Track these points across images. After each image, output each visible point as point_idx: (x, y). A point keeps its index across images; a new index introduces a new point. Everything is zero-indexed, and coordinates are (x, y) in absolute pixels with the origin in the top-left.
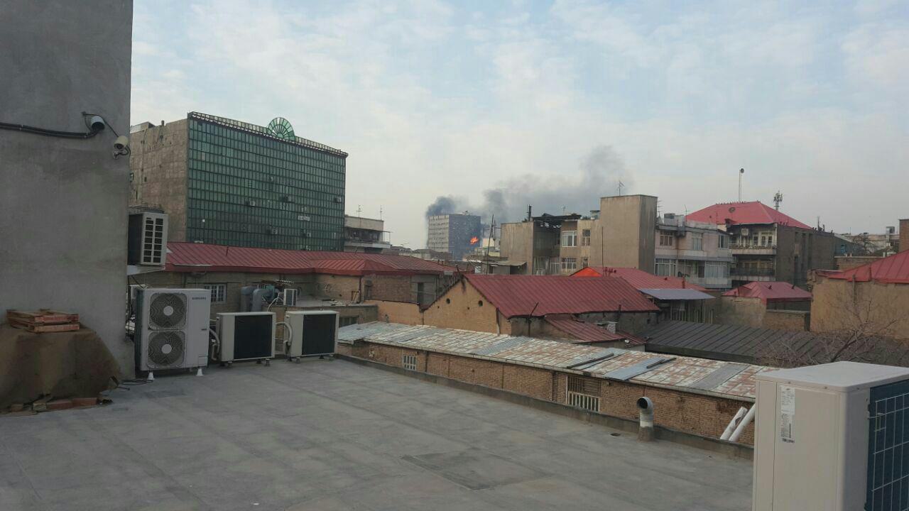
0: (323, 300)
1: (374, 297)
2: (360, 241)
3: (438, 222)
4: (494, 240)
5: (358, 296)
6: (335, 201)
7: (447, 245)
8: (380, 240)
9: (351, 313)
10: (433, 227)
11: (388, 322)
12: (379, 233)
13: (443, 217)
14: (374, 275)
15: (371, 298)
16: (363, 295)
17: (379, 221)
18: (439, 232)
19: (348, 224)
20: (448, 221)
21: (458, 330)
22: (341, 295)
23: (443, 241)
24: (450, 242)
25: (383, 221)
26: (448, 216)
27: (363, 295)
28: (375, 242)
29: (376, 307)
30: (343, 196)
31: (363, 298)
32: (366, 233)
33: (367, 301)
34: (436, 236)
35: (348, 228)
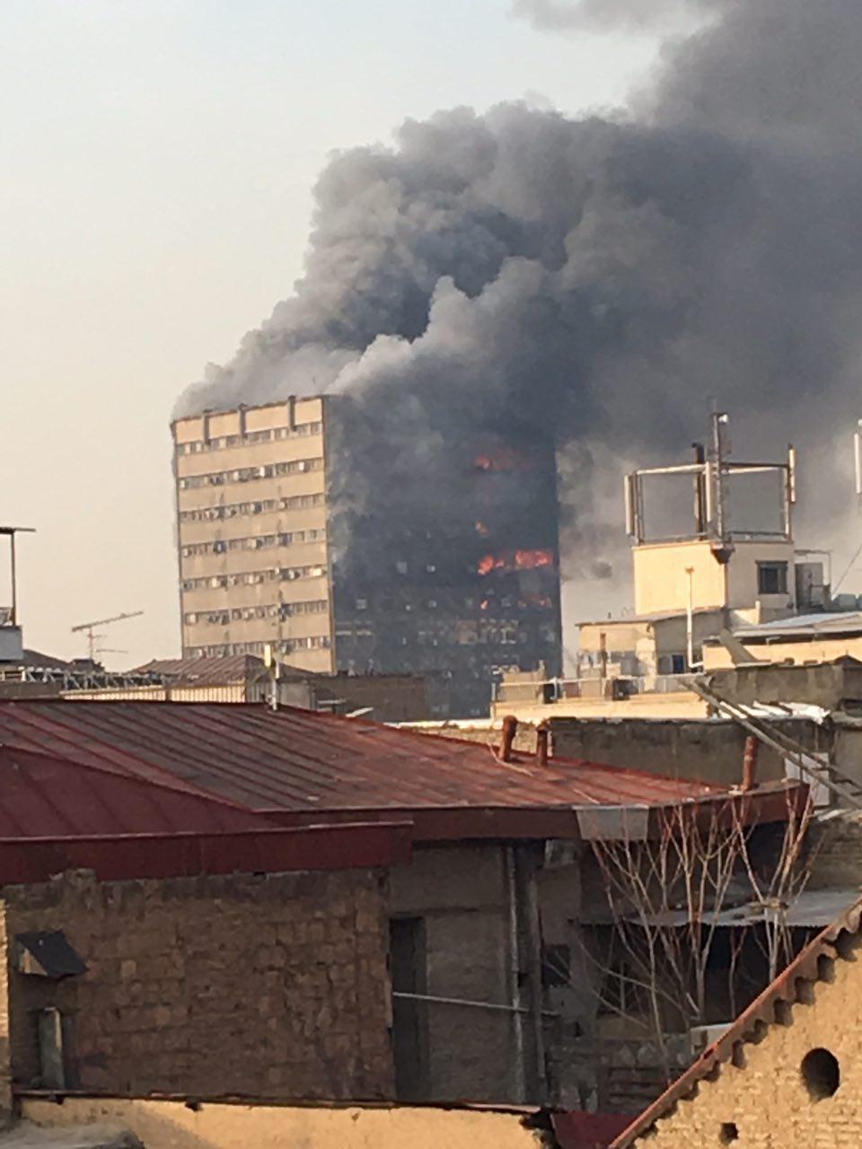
1: (91, 1075)
3: (242, 457)
4: (721, 556)
7: (319, 624)
13: (280, 417)
14: (82, 879)
18: (258, 526)
20: (313, 446)
23: (292, 593)
24: (342, 601)
26: (310, 413)
33: (33, 1108)
34: (235, 562)
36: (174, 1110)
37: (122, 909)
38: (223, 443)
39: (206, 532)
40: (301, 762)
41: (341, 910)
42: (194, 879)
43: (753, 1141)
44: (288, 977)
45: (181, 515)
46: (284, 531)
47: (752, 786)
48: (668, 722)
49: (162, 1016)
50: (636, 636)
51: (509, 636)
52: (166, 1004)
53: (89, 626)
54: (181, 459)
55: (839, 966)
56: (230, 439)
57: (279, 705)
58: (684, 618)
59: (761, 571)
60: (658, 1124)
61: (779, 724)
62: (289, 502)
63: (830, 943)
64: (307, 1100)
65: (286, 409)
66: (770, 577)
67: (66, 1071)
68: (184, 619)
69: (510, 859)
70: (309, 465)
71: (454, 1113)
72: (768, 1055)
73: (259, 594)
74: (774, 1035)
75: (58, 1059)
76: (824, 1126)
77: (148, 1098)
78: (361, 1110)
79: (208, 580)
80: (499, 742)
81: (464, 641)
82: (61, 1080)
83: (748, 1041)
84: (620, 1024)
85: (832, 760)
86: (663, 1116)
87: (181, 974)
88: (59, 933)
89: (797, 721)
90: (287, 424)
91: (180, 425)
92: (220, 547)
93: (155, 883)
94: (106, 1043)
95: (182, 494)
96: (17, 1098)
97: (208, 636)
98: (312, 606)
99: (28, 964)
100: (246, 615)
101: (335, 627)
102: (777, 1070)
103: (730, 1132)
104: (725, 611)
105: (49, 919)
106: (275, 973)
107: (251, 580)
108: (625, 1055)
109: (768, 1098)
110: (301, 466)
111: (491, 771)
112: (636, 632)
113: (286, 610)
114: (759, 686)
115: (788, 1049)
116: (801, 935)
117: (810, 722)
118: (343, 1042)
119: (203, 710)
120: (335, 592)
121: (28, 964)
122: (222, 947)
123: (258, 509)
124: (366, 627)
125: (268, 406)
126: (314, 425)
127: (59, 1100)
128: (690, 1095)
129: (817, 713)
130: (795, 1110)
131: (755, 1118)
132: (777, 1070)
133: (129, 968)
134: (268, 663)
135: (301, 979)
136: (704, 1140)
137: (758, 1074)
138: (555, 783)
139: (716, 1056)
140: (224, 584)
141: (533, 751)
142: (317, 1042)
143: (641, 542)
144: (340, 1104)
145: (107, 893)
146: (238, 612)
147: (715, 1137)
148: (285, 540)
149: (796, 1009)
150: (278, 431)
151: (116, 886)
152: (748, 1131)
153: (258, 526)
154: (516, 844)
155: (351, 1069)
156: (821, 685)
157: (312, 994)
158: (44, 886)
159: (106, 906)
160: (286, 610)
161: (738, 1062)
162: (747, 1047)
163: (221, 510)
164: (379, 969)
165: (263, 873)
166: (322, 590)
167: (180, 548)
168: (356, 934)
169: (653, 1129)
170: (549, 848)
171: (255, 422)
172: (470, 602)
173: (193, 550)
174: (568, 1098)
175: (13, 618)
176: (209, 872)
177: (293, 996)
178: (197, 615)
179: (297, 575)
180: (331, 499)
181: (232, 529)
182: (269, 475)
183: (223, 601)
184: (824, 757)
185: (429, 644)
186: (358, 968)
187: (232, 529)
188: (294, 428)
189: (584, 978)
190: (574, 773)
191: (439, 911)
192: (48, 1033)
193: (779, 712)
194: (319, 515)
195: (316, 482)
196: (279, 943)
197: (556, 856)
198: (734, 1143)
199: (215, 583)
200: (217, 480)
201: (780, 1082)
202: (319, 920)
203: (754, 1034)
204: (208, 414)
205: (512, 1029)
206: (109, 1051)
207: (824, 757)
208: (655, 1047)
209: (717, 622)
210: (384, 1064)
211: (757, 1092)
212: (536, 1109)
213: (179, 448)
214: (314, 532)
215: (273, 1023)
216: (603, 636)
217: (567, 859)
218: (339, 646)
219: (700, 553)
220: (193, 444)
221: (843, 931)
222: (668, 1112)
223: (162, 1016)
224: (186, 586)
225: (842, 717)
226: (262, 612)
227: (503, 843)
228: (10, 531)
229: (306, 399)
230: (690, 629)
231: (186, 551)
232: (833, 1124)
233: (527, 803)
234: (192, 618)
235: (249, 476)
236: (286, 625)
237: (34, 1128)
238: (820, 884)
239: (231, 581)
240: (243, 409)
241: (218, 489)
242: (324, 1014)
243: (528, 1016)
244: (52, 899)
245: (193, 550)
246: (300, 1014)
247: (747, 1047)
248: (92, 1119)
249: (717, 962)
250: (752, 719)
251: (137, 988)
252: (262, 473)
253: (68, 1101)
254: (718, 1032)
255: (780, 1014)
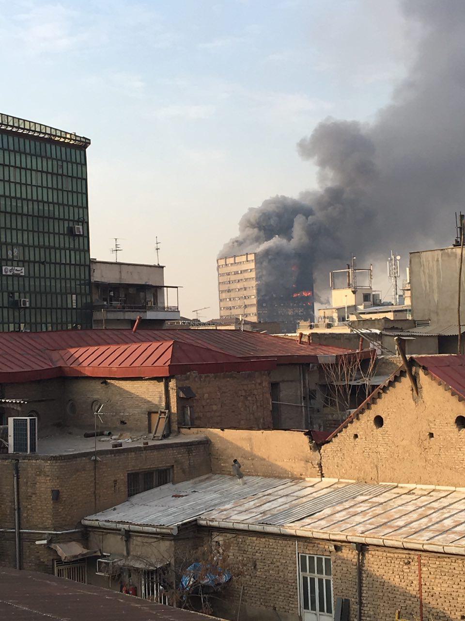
0: (87, 436)
1: (197, 422)
2: (123, 309)
3: (235, 268)
4: (354, 292)
5: (163, 423)
6: (71, 232)
7: (254, 310)
8: (159, 305)
9: (156, 461)
10: (225, 278)
11: (241, 476)
12: (157, 290)
13: (244, 258)
14: (194, 374)
15: (193, 425)
16: (174, 418)
17: (154, 266)
18: (239, 286)
19: (98, 276)
20: (252, 265)
21: (411, 486)
22: (123, 423)
23: (247, 302)
24: (260, 304)
25: (163, 267)
26: (251, 257)
27: (174, 418)
28: (151, 309)
29: (206, 443)
30: (85, 223)
31: (175, 426)
32: (131, 291)
33: (183, 430)
34: (233, 294)
35: (98, 285)
36: (217, 431)
37: (204, 381)
38: (230, 265)
39: (226, 287)
40: (249, 344)
41: (259, 381)
42: (222, 374)
43: (362, 438)
44: (246, 398)
45: (219, 283)
46: (245, 286)
47: (362, 350)
48: (340, 334)
49: (215, 408)
50: (333, 312)
51: (301, 312)
52: (216, 405)
53: (197, 311)
54: (220, 269)
55: (383, 395)
56: (232, 264)
57: (244, 330)
58: (345, 308)
59: (364, 296)
60: (338, 434)
61: (368, 334)
62: (246, 279)
63: (381, 389)
64: (251, 429)
65: (246, 256)
66: (366, 297)
67: (191, 421)
68: (220, 308)
69: (301, 369)
70: (251, 270)
71: (287, 432)
72: (366, 417)
73: (239, 303)
74: (367, 412)
75: (189, 418)
76: (379, 435)
77: (212, 428)
78: (264, 431)
79: (226, 299)
80: (298, 339)
81: (290, 314)
82: (190, 424)
83: (360, 413)
84: (329, 409)
85: (382, 343)
86: (339, 432)
87: (219, 397)
88: (189, 387)
89: (373, 334)
90: (246, 260)
91: (219, 261)
92: (229, 291)
93: (213, 374)
94: (201, 414)
95: (220, 278)
96: (179, 428)
97: (226, 313)
98: (252, 305)
99: (182, 395)
100: (236, 308)
101: (258, 311)
102: (368, 421)
103: (356, 436)
104: (355, 306)
105: (187, 383)
106: (242, 397)
107: (237, 299)
108: (330, 417)
109: (366, 428)
110: (249, 271)
111: (297, 346)
112: (332, 311)
113: (246, 306)
114: (363, 325)
115: (371, 415)
116: (374, 387)
117: (376, 334)
118: (259, 414)
119: (224, 332)
120: (258, 302)
121: (182, 395)
122: (229, 391)
123: (239, 281)
124: (266, 311)
125: (241, 256)
126: (252, 260)
127: (189, 428)
128: (346, 427)
129: (378, 332)
130: (372, 431)
131: (362, 433)
132: (368, 421)
133: (206, 396)
134: (241, 320)
135: (249, 398)
136: (350, 438)
137: (363, 422)
138: (312, 349)
139: (352, 417)
140: (230, 300)
141: (307, 341)
142: (253, 414)
143: (334, 289)
144: (259, 429)
145: (201, 377)
146: (234, 307)
147: (352, 437)
148: (245, 289)
149: (372, 406)
150: (243, 262)
151: (203, 376)
152: (361, 436)
153: (239, 286)
154: (303, 364)
155: (262, 420)
156: (379, 324)
157: (251, 402)
158: (185, 375)
159: (200, 380)
160: (246, 306)
161: (358, 419)
162: (360, 415)
163: (229, 281)
164: (268, 396)
165: (239, 372)
166: (254, 301)
167: (219, 291)
168: (263, 387)
169: (337, 435)
170: (311, 365)
171: (238, 259)
172: (291, 304)
173: (222, 292)
174: (316, 427)
175: (178, 309)
176: (226, 371)
177: (247, 403)
178: (224, 308)
179: (248, 298)
180: (257, 279)
181: (232, 286)
182: (241, 273)
183: (230, 304)
184: (380, 342)
185: (281, 315)
186: (263, 395)
187: (232, 286)
188: (248, 261)
189: (320, 397)
190: (317, 347)
191: (283, 381)
192: (187, 412)
193: (368, 331)
194: (254, 283)
195: (253, 275)
196: (244, 389)
197: (313, 367)
198: (357, 439)
199: (228, 300)
200: (228, 274)
201: (369, 424)
202: (253, 384)
203: (362, 412)
204: (226, 258)
205: (302, 411)
206: (202, 416)
207: (380, 342)
208: (337, 415)
209: (353, 309)
210: (270, 419)
211: (363, 426)
212: (307, 431)
213: (219, 267)
214: (253, 287)
215: (242, 409)
216: (325, 312)
217: (315, 368)
218: (259, 315)
219: (349, 292)
220: (222, 265)
221: (384, 386)
222: (341, 431)
223: (215, 408)
224: (221, 300)
225: (384, 332)
226: (240, 307)
227: (299, 364)
228: (177, 287)
229: (251, 254)
230: (346, 310)
231: (221, 292)
232: (382, 434)
233: (305, 354)
234: (222, 309)
235: (236, 273)
236: (245, 310)
237: (183, 435)
238: (379, 374)
239: (232, 299)
240: (235, 257)
241: (229, 277)
242: (255, 407)
243: (306, 407)
244: (187, 378)
245: (222, 292)
246: (249, 407)
247: (360, 415)
248: (197, 433)
249: (353, 394)
250: (361, 333)
251: (208, 401)
252: (240, 272)
253: (191, 429)
254: (353, 411)
255: (368, 407)
